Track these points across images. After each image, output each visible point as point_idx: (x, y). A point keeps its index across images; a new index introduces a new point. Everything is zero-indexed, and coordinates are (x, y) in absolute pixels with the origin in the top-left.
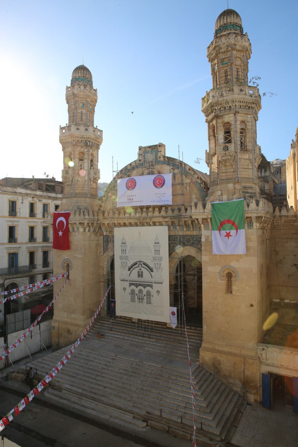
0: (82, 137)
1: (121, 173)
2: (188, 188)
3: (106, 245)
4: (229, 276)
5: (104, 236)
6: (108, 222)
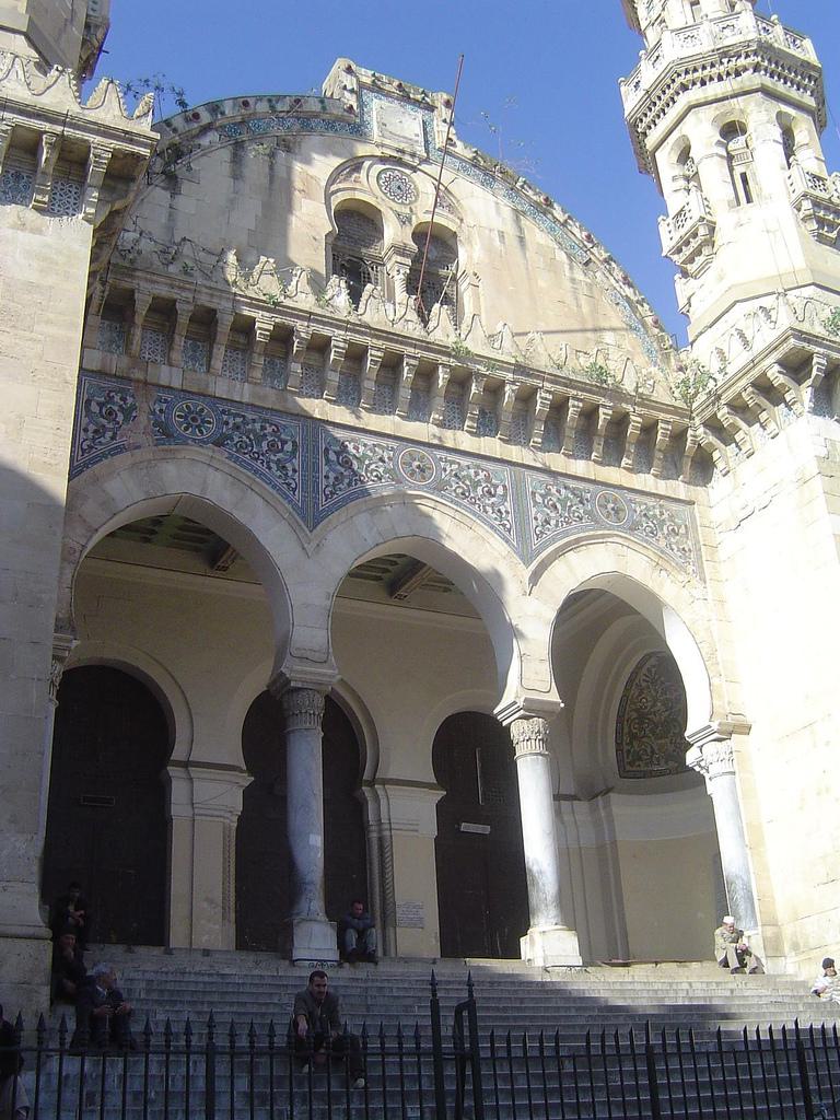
3: (92, 427)
6: (163, 291)
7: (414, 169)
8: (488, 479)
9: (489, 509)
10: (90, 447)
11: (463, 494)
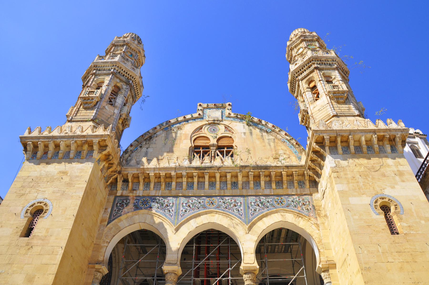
0: (126, 71)
1: (167, 124)
2: (272, 144)
3: (117, 210)
4: (385, 209)
5: (116, 197)
7: (219, 124)
8: (235, 201)
9: (235, 210)
10: (116, 215)
11: (226, 207)
